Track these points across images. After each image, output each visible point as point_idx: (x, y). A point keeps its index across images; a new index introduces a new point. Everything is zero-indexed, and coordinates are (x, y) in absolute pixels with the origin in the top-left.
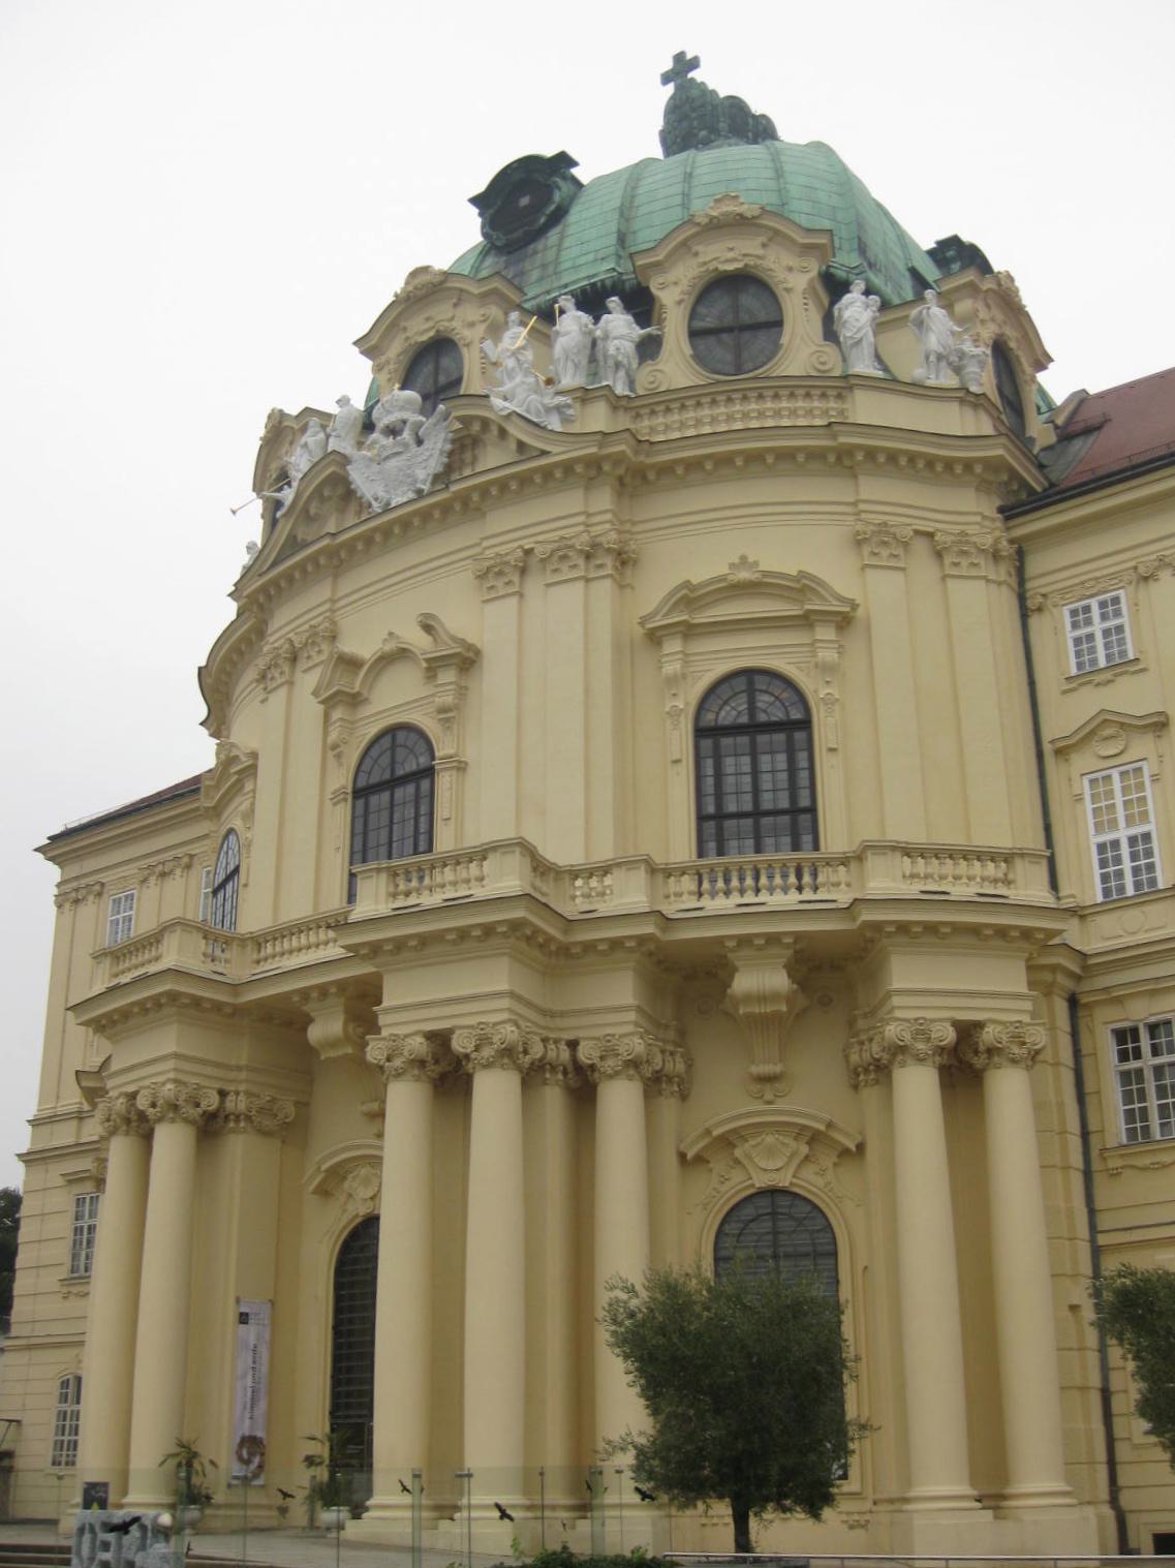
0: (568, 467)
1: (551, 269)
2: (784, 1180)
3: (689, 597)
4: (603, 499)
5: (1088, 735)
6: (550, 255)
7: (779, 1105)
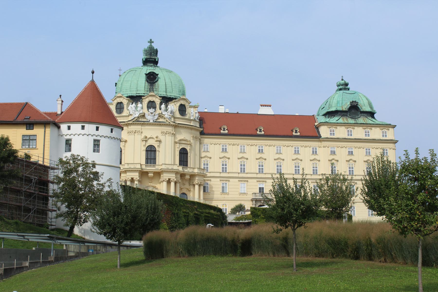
0: (172, 125)
1: (157, 90)
2: (185, 192)
3: (180, 140)
4: (173, 128)
5: (204, 157)
6: (157, 87)
7: (185, 186)
